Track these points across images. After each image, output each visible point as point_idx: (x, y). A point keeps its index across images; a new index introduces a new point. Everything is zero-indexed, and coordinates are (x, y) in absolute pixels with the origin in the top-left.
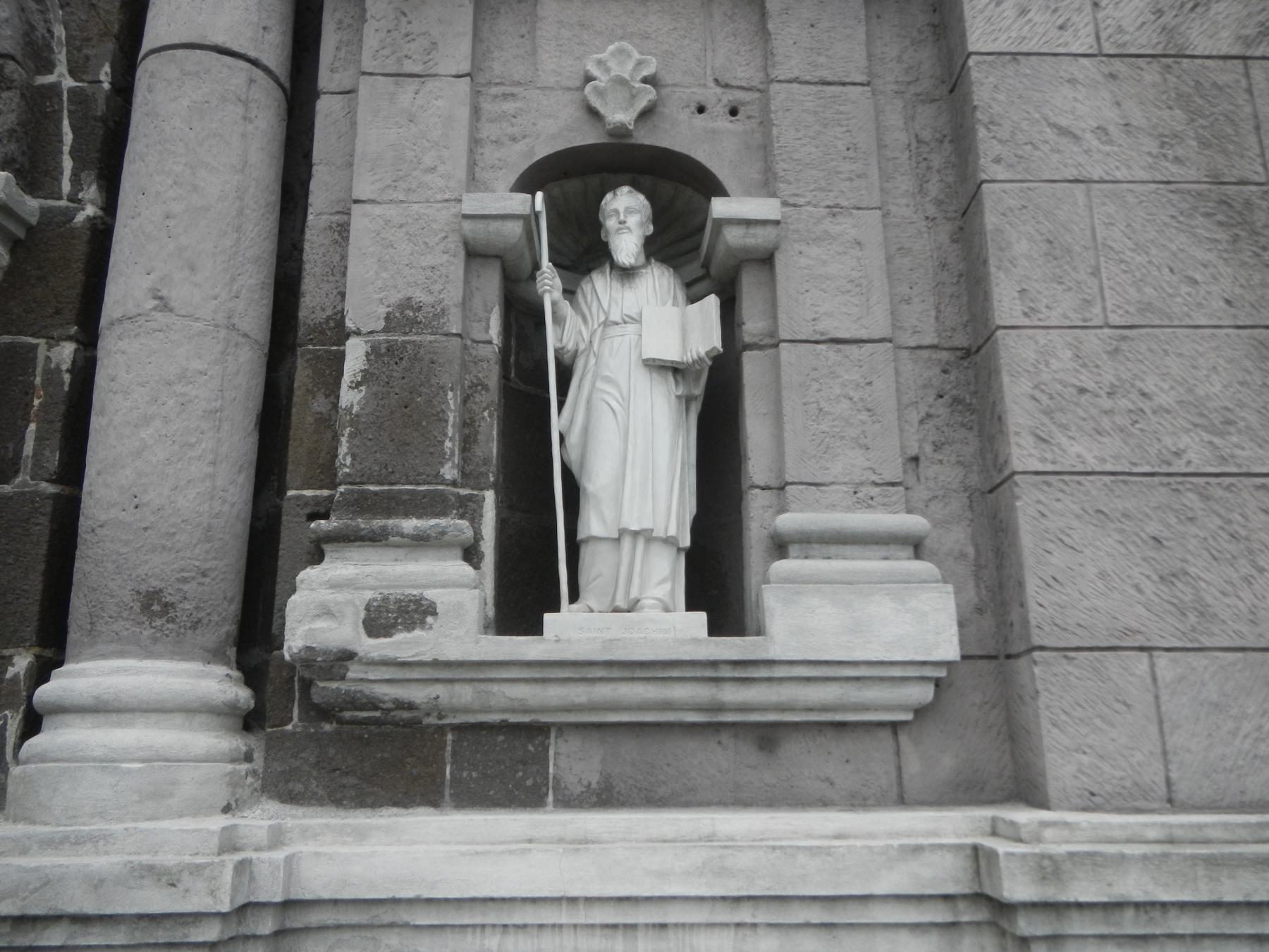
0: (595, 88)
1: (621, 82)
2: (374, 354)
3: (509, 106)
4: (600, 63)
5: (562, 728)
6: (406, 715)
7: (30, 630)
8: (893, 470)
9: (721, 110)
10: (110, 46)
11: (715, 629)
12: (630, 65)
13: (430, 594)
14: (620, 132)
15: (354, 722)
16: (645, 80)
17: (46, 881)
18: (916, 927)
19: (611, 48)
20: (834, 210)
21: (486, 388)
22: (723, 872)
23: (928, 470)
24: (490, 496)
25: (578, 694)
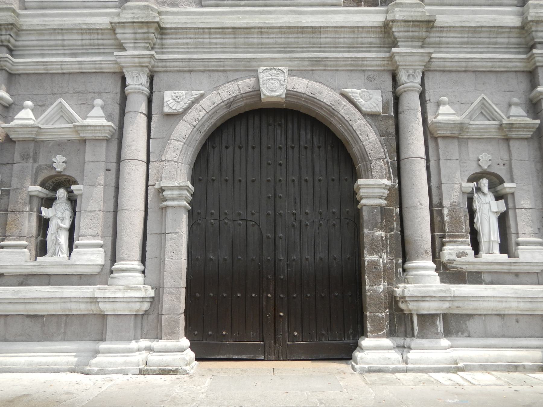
0: (481, 162)
1: (485, 160)
2: (449, 211)
3: (465, 164)
5: (484, 272)
7: (401, 255)
8: (537, 231)
10: (396, 154)
11: (509, 257)
12: (487, 157)
13: (466, 251)
16: (490, 160)
17: (427, 291)
19: (483, 154)
20: (524, 185)
21: (467, 216)
22: (516, 293)
24: (469, 234)
25: (489, 267)
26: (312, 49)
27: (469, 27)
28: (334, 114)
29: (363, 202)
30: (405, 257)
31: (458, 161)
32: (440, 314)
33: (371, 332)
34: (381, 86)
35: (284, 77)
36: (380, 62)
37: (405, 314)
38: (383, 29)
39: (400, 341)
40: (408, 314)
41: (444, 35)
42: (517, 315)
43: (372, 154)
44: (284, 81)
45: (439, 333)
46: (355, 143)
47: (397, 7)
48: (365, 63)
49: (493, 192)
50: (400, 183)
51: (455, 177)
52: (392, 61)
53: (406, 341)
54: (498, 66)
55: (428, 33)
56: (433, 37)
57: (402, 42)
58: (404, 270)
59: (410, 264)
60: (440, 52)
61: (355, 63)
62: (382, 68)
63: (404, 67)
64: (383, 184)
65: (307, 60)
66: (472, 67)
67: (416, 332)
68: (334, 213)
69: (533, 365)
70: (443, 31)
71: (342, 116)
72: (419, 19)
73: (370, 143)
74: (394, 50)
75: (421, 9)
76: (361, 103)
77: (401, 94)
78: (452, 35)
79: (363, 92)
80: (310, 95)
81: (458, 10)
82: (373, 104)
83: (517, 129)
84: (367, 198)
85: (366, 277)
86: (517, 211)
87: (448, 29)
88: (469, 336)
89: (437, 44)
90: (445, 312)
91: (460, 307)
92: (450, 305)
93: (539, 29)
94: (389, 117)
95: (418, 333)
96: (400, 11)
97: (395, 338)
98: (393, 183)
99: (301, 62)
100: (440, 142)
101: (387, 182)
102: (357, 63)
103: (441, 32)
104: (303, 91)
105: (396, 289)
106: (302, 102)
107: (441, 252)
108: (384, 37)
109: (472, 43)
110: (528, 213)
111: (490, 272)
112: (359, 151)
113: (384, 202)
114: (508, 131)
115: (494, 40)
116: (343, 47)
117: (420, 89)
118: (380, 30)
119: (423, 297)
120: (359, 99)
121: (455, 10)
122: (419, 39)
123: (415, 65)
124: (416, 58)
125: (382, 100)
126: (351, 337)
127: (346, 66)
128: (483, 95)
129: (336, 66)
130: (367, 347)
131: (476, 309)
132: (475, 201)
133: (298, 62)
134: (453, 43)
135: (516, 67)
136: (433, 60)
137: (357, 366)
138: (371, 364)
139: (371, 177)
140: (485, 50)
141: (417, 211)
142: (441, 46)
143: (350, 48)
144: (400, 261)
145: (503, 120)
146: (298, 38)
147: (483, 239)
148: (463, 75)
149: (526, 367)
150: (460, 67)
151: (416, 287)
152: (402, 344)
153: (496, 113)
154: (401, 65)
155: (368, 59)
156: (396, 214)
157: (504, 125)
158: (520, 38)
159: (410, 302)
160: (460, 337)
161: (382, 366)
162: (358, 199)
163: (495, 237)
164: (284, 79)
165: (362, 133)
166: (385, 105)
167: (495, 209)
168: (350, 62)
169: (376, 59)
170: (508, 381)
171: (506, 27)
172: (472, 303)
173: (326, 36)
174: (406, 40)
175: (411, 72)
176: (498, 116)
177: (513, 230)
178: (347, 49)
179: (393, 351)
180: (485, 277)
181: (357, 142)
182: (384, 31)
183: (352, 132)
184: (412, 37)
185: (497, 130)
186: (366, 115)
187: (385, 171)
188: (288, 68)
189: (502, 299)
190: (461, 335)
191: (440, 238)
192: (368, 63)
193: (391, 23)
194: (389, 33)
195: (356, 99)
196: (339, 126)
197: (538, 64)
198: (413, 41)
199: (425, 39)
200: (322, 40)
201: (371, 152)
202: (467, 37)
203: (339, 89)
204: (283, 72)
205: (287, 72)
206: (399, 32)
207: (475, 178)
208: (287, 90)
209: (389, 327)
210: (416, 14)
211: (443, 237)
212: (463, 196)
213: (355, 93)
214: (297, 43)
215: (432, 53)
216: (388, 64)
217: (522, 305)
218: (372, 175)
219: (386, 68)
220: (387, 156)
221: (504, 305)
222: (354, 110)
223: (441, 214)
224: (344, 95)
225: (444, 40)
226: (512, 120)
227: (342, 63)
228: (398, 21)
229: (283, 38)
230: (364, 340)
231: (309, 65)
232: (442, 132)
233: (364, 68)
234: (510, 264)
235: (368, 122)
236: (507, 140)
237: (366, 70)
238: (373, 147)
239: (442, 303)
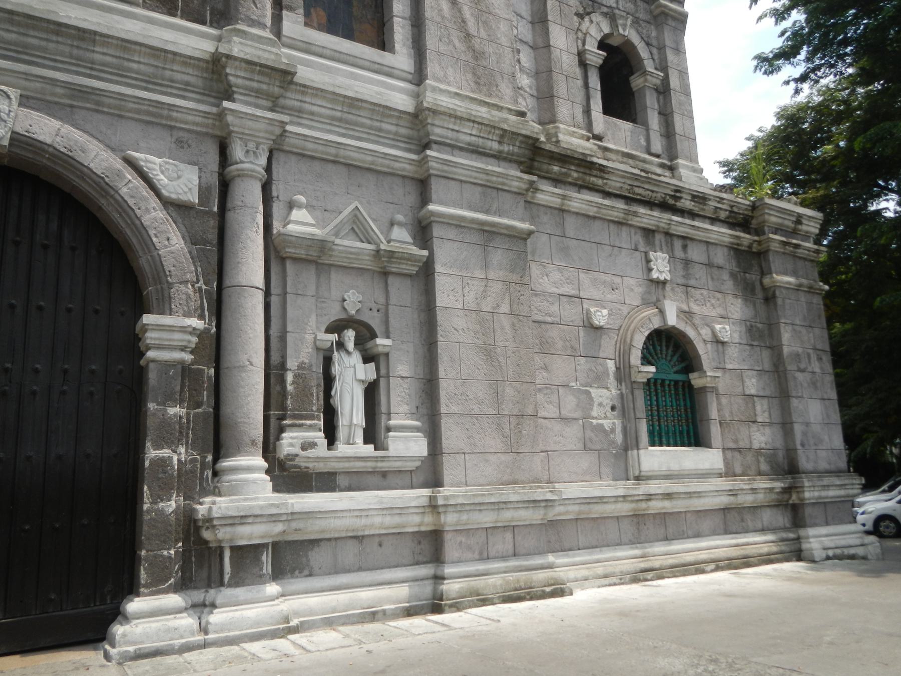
2: (295, 376)
3: (323, 305)
4: (348, 296)
5: (340, 473)
6: (306, 470)
8: (414, 411)
9: (376, 310)
11: (375, 449)
13: (316, 440)
14: (352, 316)
15: (293, 472)
17: (251, 507)
18: (417, 513)
20: (403, 342)
22: (382, 503)
23: (420, 410)
25: (347, 465)
26: (74, 68)
27: (345, 97)
28: (107, 193)
29: (151, 354)
30: (219, 451)
31: (313, 300)
32: (268, 544)
33: (147, 586)
34: (200, 159)
35: (9, 106)
36: (200, 118)
37: (210, 548)
38: (211, 66)
39: (198, 596)
40: (216, 548)
41: (308, 99)
42: (380, 535)
43: (173, 273)
44: (8, 115)
45: (264, 574)
46: (143, 249)
47: (237, 36)
48: (175, 114)
49: (360, 351)
50: (219, 326)
51: (307, 324)
52: (221, 121)
53: (208, 595)
54: (381, 164)
55: (282, 91)
56: (291, 99)
57: (241, 94)
58: (215, 474)
59: (226, 463)
60: (299, 124)
61: (154, 110)
62: (204, 130)
63: (241, 136)
64: (190, 326)
65: (63, 85)
66: (344, 158)
67: (227, 578)
68: (93, 372)
69: (396, 608)
70: (307, 93)
71: (122, 198)
72: (269, 63)
73: (172, 253)
74: (226, 104)
75: (274, 50)
76: (161, 182)
77: (233, 178)
78: (319, 102)
79: (167, 163)
80: (63, 150)
81: (332, 67)
82: (182, 186)
83: (399, 261)
84: (159, 347)
85: (146, 488)
86: (391, 379)
87: (315, 92)
88: (310, 575)
89: (296, 111)
90: (276, 539)
91: (300, 530)
92: (285, 528)
93: (437, 122)
94: (209, 213)
95: (230, 578)
96: (241, 43)
97: (189, 592)
98: (206, 326)
99: (48, 87)
100: (290, 267)
101: (196, 323)
102: (160, 111)
103: (303, 93)
104: (48, 140)
105: (198, 507)
106: (44, 161)
107: (278, 443)
108: (211, 80)
109: (347, 122)
110: (405, 384)
111: (348, 472)
112: (151, 266)
113: (188, 357)
114: (388, 262)
115: (378, 124)
116: (136, 79)
117: (264, 176)
118: (205, 65)
119: (242, 517)
120: (157, 175)
121: (327, 65)
122: (268, 96)
123: (258, 137)
124: (261, 126)
125: (200, 183)
126: (108, 598)
127: (138, 112)
128: (356, 203)
129: (119, 108)
130: (136, 613)
131: (323, 531)
132: (334, 363)
133: (43, 85)
134: (320, 115)
135: (404, 170)
136: (287, 134)
137: (113, 652)
138: (142, 642)
139: (168, 312)
140: (365, 136)
141: (244, 375)
142: (301, 115)
143: (149, 83)
144: (210, 458)
145: (381, 245)
146: (47, 40)
147: (342, 422)
148: (330, 166)
149: (387, 613)
150: (327, 154)
151: (231, 501)
152: (202, 600)
153: (373, 234)
154: (237, 132)
155: (180, 109)
156: (209, 377)
157: (382, 252)
158: (412, 129)
159: (219, 527)
160: (297, 577)
161: (162, 643)
162: (142, 349)
163: (359, 418)
164: (10, 111)
165: (158, 235)
166: (204, 192)
167: (361, 376)
168: (145, 108)
169: (194, 113)
170: (359, 638)
171: (395, 110)
172: (318, 522)
173: (105, 50)
174: (247, 92)
175: (251, 146)
176: (375, 237)
177: (383, 409)
178: (144, 84)
179: (185, 615)
180: (342, 481)
181: (148, 248)
182: (213, 70)
183: (141, 230)
184: (258, 91)
185: (372, 259)
186: (168, 204)
187: (194, 304)
188: (19, 91)
189: (362, 513)
190: (299, 575)
191: (278, 419)
192: (179, 115)
193: (224, 59)
194: (220, 75)
195: (153, 174)
196: (117, 216)
197: (431, 171)
198: (258, 97)
199: (277, 98)
200: (97, 57)
201: (172, 269)
202: (341, 111)
203: (122, 151)
204: (8, 97)
205: (16, 98)
206: (237, 76)
207: (337, 327)
208: (13, 132)
209: (180, 574)
210: (266, 55)
211: (282, 418)
212: (317, 354)
213: (153, 163)
214: (45, 50)
215: (287, 123)
216: (214, 125)
217: (389, 520)
218: (171, 309)
219: (210, 131)
220: (201, 278)
221: (364, 521)
222: (147, 192)
223: (282, 381)
224: (131, 163)
225: (307, 106)
226: (394, 247)
227: (131, 105)
228: (236, 59)
229: (15, 32)
230: (132, 601)
231: (64, 95)
232: (293, 251)
233: (173, 124)
234: (376, 459)
235: (171, 216)
236: (385, 274)
237: (175, 127)
238: (176, 260)
239: (273, 524)
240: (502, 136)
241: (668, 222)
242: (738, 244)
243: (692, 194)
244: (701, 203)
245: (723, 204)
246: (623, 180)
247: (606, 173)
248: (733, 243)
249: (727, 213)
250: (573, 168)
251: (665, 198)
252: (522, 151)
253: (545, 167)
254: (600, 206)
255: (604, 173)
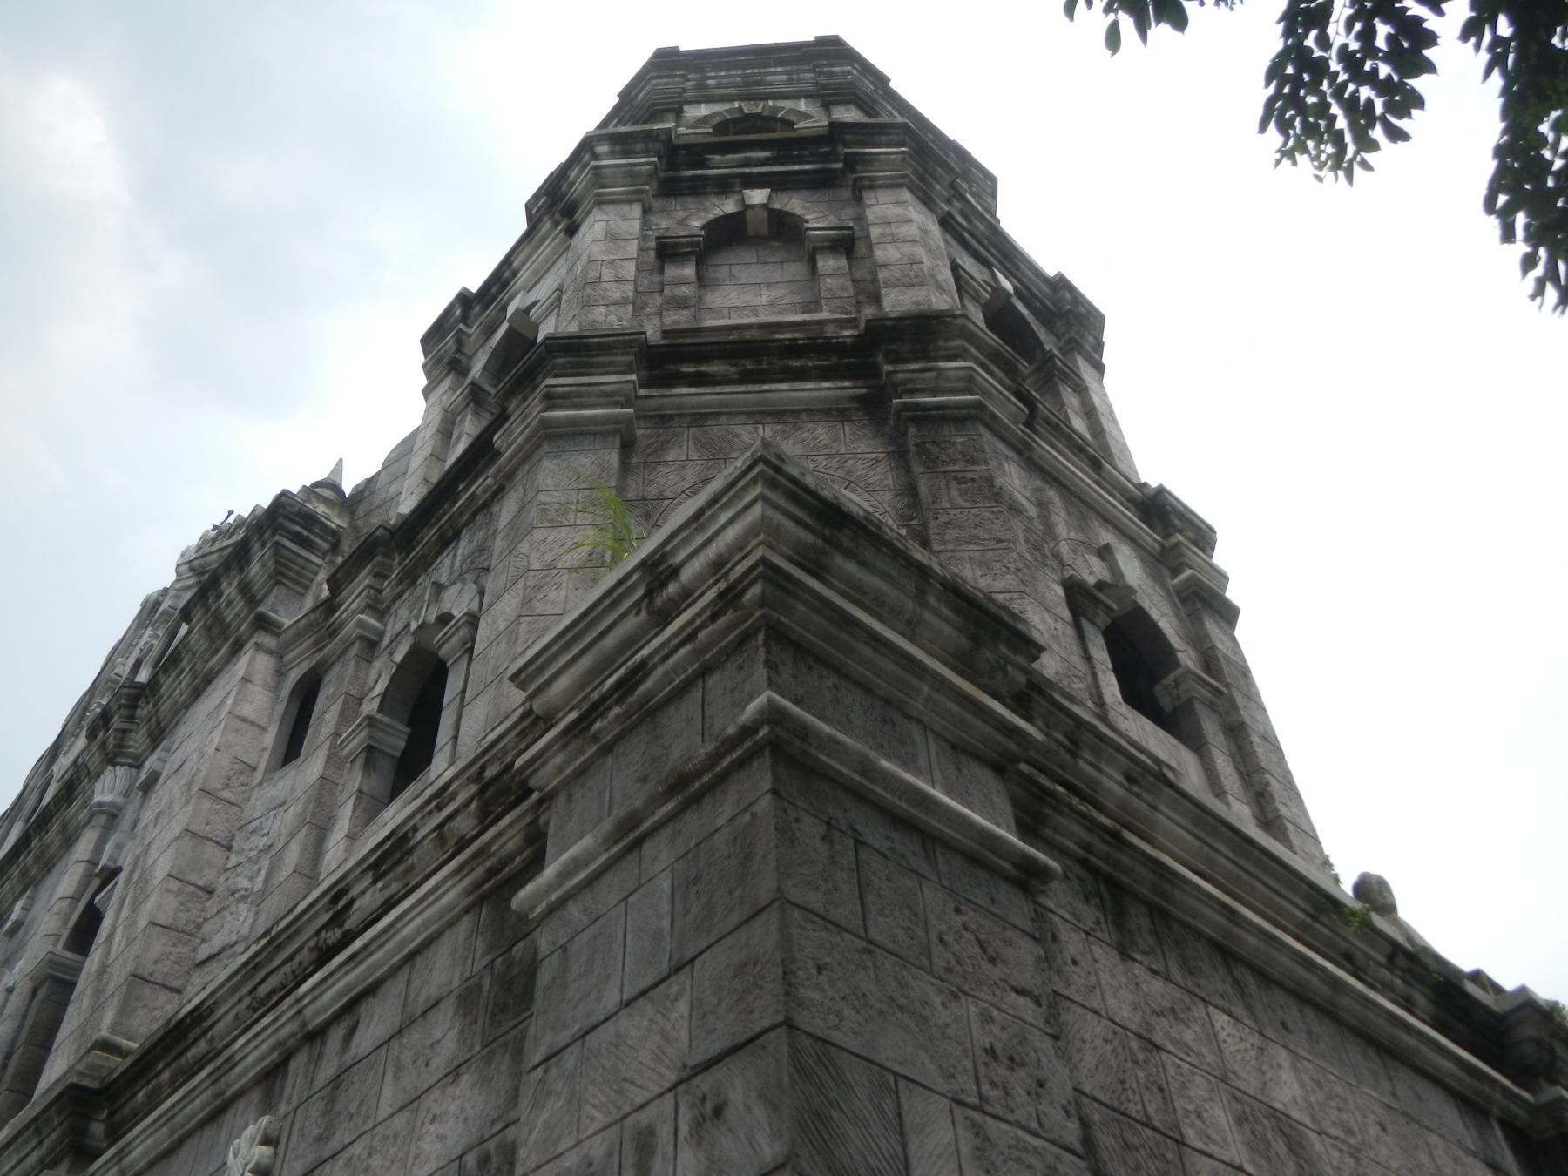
240: (38, 1131)
241: (294, 1011)
242: (492, 872)
243: (369, 868)
244: (400, 861)
245: (453, 797)
246: (235, 999)
247: (210, 1015)
248: (477, 885)
249: (474, 805)
250: (161, 1066)
251: (317, 943)
252: (65, 1125)
253: (126, 1111)
254: (169, 1116)
255: (206, 1018)
